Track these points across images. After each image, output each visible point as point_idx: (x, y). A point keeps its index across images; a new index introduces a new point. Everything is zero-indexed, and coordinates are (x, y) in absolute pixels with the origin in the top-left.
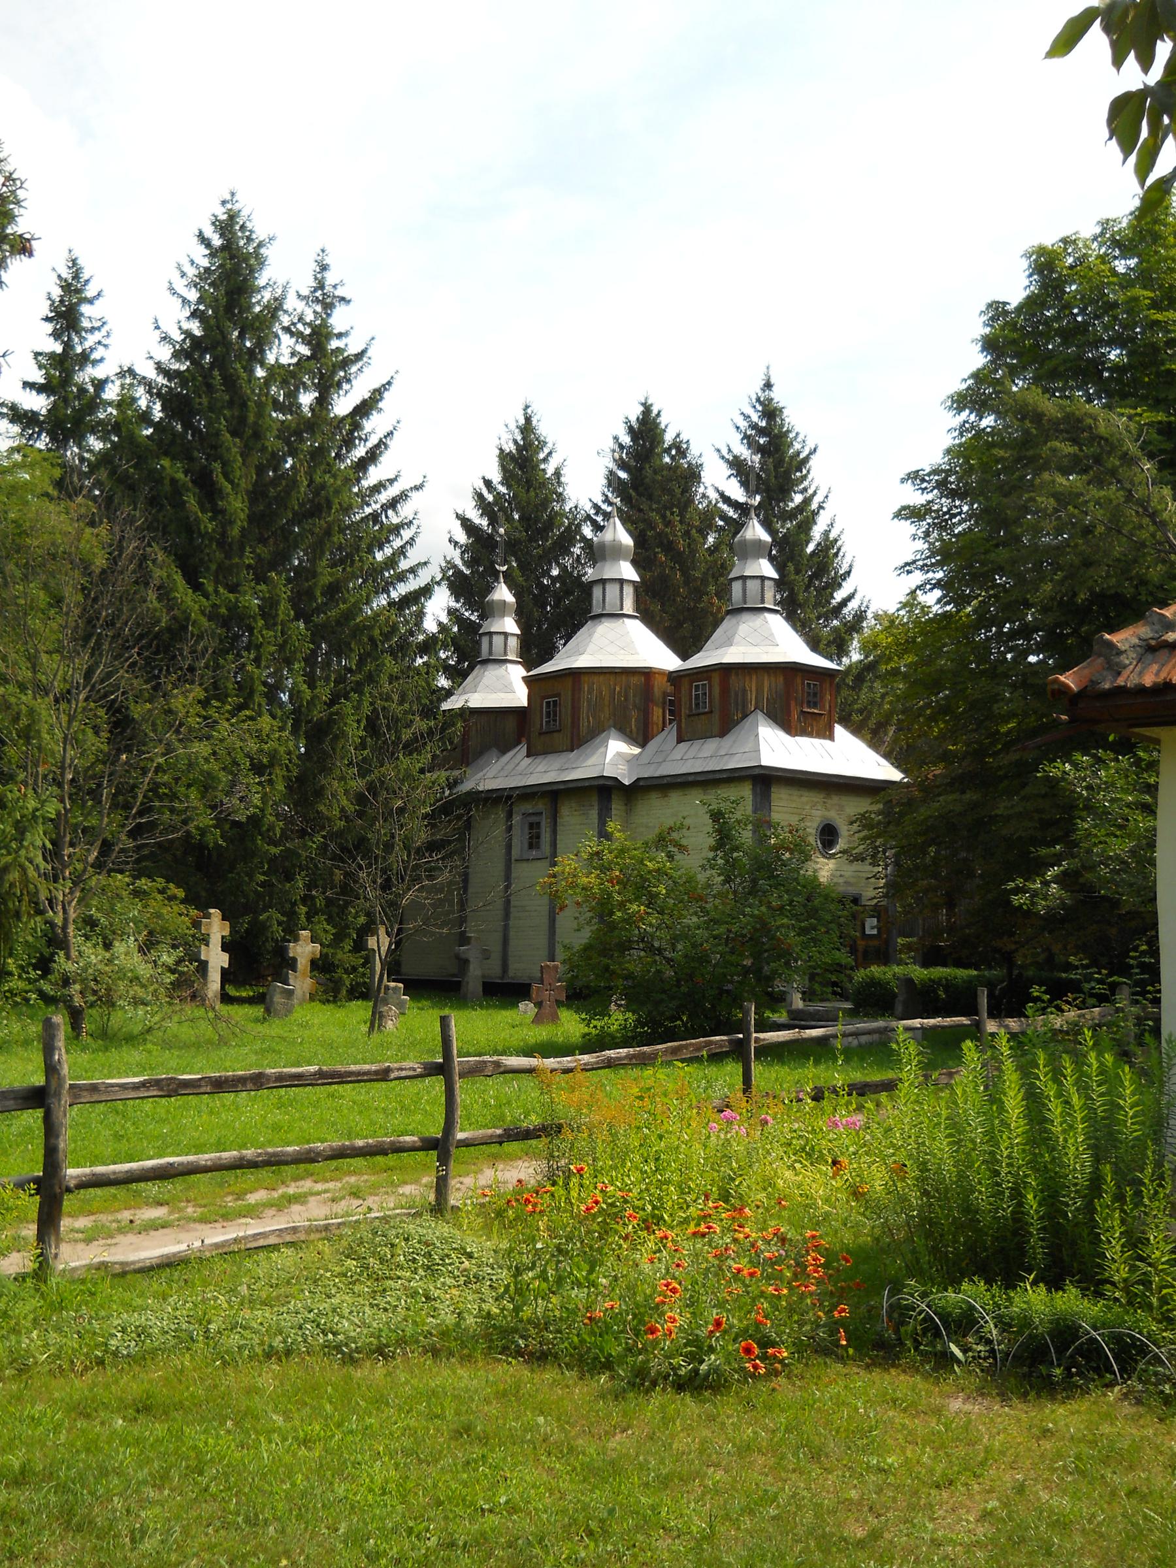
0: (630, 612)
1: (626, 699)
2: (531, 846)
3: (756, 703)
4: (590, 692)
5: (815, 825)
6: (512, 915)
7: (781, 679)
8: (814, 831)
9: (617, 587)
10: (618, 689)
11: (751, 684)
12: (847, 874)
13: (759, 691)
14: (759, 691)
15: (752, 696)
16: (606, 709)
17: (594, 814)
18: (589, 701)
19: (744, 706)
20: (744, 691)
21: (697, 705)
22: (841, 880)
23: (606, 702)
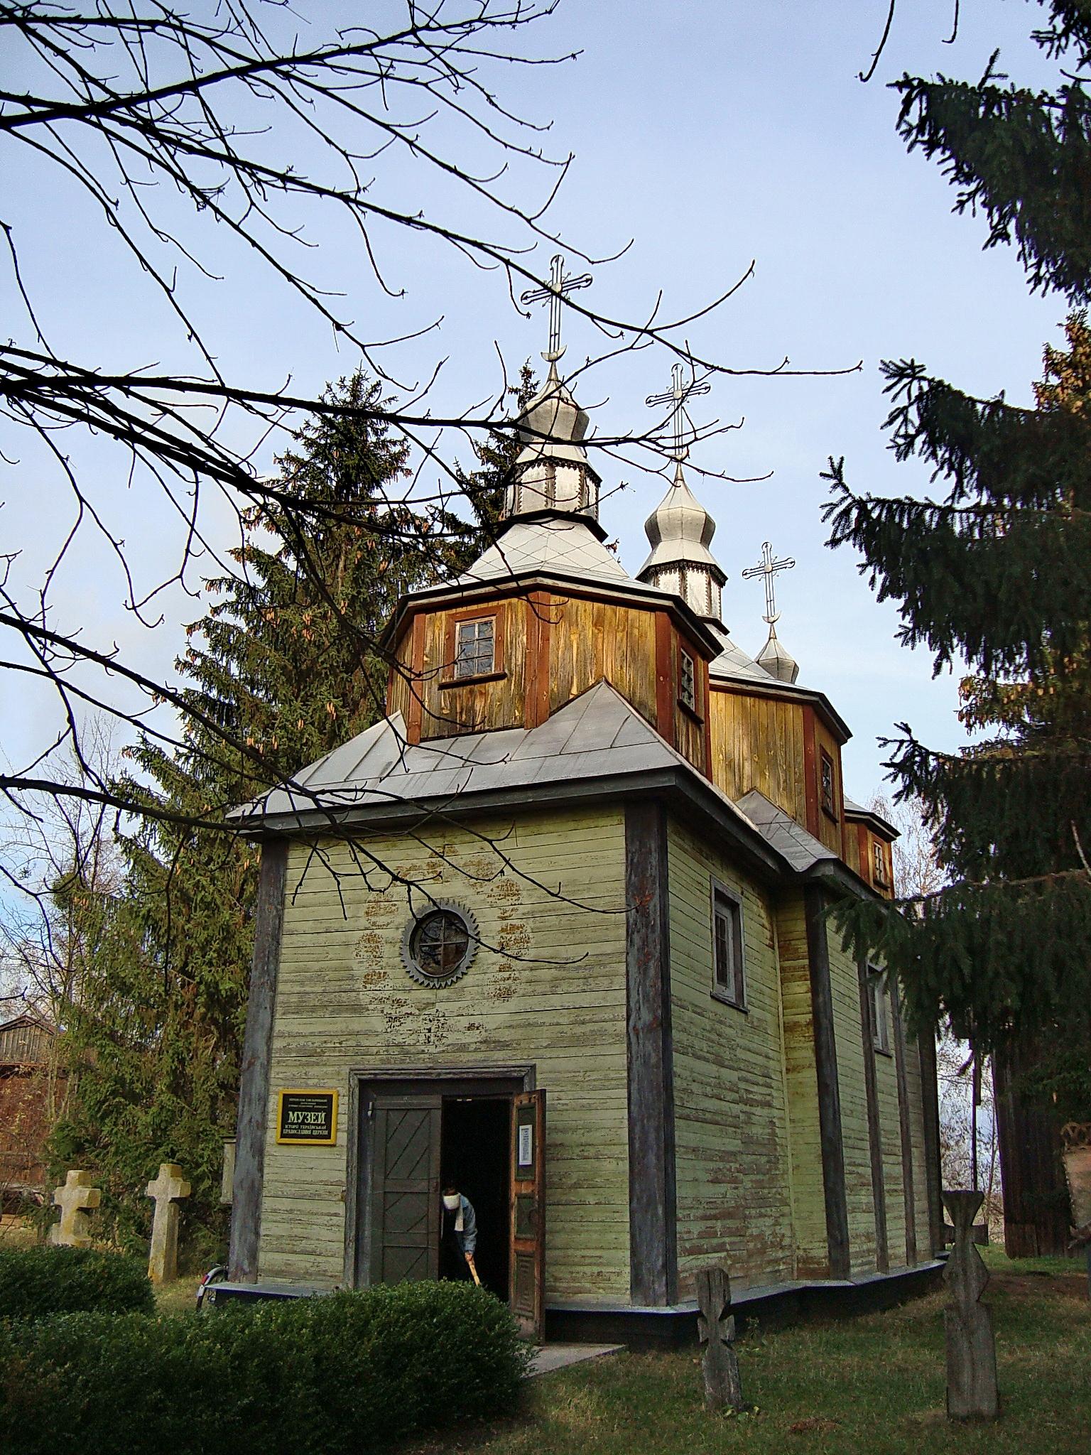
12: (491, 1022)
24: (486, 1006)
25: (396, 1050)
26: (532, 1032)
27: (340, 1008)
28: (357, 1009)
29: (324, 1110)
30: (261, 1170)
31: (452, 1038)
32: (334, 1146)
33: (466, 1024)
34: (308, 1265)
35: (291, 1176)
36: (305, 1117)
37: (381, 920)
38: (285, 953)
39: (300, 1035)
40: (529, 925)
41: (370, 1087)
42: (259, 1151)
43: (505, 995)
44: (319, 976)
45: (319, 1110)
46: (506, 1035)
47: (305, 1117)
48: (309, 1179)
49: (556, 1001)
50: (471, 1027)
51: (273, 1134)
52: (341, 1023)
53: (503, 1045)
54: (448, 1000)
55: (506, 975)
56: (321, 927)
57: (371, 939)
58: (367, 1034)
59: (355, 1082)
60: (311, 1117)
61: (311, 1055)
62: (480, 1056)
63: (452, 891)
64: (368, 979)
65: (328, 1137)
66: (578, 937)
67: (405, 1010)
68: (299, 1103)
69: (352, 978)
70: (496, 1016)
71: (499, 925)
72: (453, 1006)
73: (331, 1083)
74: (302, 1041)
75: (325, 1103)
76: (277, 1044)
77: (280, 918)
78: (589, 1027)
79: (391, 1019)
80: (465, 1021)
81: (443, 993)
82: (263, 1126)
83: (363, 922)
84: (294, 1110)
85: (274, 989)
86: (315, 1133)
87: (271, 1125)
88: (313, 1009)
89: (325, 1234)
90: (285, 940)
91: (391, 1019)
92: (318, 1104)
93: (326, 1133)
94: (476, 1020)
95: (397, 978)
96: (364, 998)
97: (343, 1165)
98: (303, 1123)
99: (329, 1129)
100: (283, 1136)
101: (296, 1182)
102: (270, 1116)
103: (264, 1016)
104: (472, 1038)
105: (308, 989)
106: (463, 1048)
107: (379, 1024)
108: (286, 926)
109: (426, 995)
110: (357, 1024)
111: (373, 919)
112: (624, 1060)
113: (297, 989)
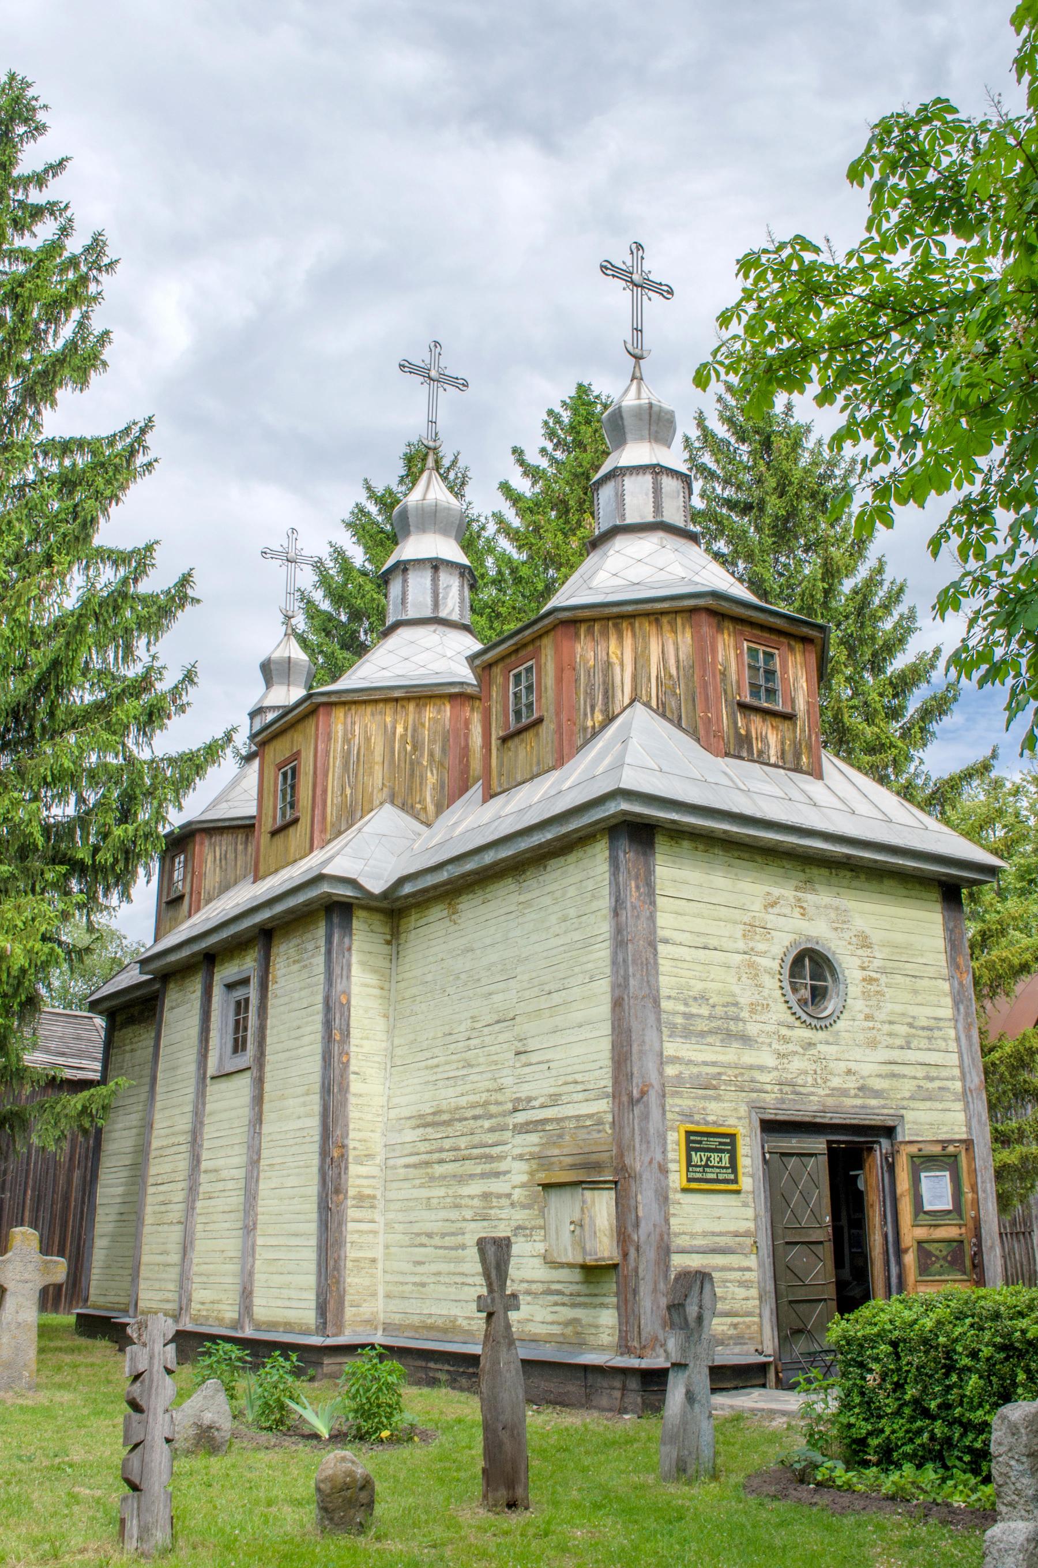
0: (455, 617)
1: (415, 747)
2: (235, 1050)
3: (635, 688)
4: (347, 740)
5: (778, 950)
6: (202, 1189)
7: (688, 635)
8: (775, 965)
9: (428, 574)
10: (400, 730)
11: (620, 652)
12: (866, 1069)
13: (640, 660)
14: (640, 660)
15: (624, 678)
16: (378, 770)
17: (319, 961)
18: (346, 756)
19: (608, 694)
20: (608, 664)
21: (518, 714)
22: (851, 1084)
23: (378, 757)
24: (857, 1053)
25: (786, 1089)
26: (894, 1083)
27: (729, 1036)
28: (745, 1039)
29: (728, 1151)
30: (667, 1221)
31: (836, 1082)
32: (738, 1192)
33: (844, 1068)
34: (725, 1328)
35: (698, 1228)
36: (708, 1159)
37: (761, 947)
38: (665, 966)
39: (690, 1062)
40: (883, 979)
41: (771, 1127)
42: (664, 1199)
43: (873, 1044)
44: (702, 998)
45: (722, 1151)
46: (878, 1084)
47: (708, 1159)
48: (717, 1229)
49: (911, 1056)
50: (849, 1072)
51: (677, 1178)
52: (730, 1054)
53: (877, 1094)
54: (828, 1043)
55: (871, 1024)
56: (701, 941)
57: (751, 965)
58: (761, 1068)
59: (757, 1124)
60: (715, 1158)
61: (707, 1086)
62: (858, 1102)
63: (820, 931)
64: (753, 1008)
65: (735, 1181)
66: (919, 999)
67: (791, 1047)
68: (700, 1142)
69: (736, 1004)
70: (868, 1064)
71: (859, 975)
72: (831, 1050)
73: (732, 1121)
74: (695, 1070)
75: (728, 1142)
76: (670, 1071)
77: (652, 918)
78: (937, 1084)
79: (781, 1056)
80: (842, 1066)
81: (821, 1035)
82: (664, 1171)
83: (741, 945)
84: (697, 1150)
85: (656, 1002)
86: (721, 1177)
87: (672, 1166)
88: (702, 1034)
89: (741, 1292)
90: (661, 948)
91: (781, 1056)
92: (721, 1143)
93: (732, 1177)
94: (853, 1066)
95: (779, 1012)
96: (752, 1029)
97: (750, 1213)
98: (707, 1166)
99: (735, 1171)
100: (689, 1180)
101: (705, 1234)
102: (671, 1155)
103: (651, 1035)
104: (851, 1084)
105: (694, 1010)
106: (844, 1093)
107: (770, 1061)
108: (661, 933)
109: (806, 1034)
110: (749, 1057)
111: (751, 944)
112: (961, 1117)
113: (682, 1008)
